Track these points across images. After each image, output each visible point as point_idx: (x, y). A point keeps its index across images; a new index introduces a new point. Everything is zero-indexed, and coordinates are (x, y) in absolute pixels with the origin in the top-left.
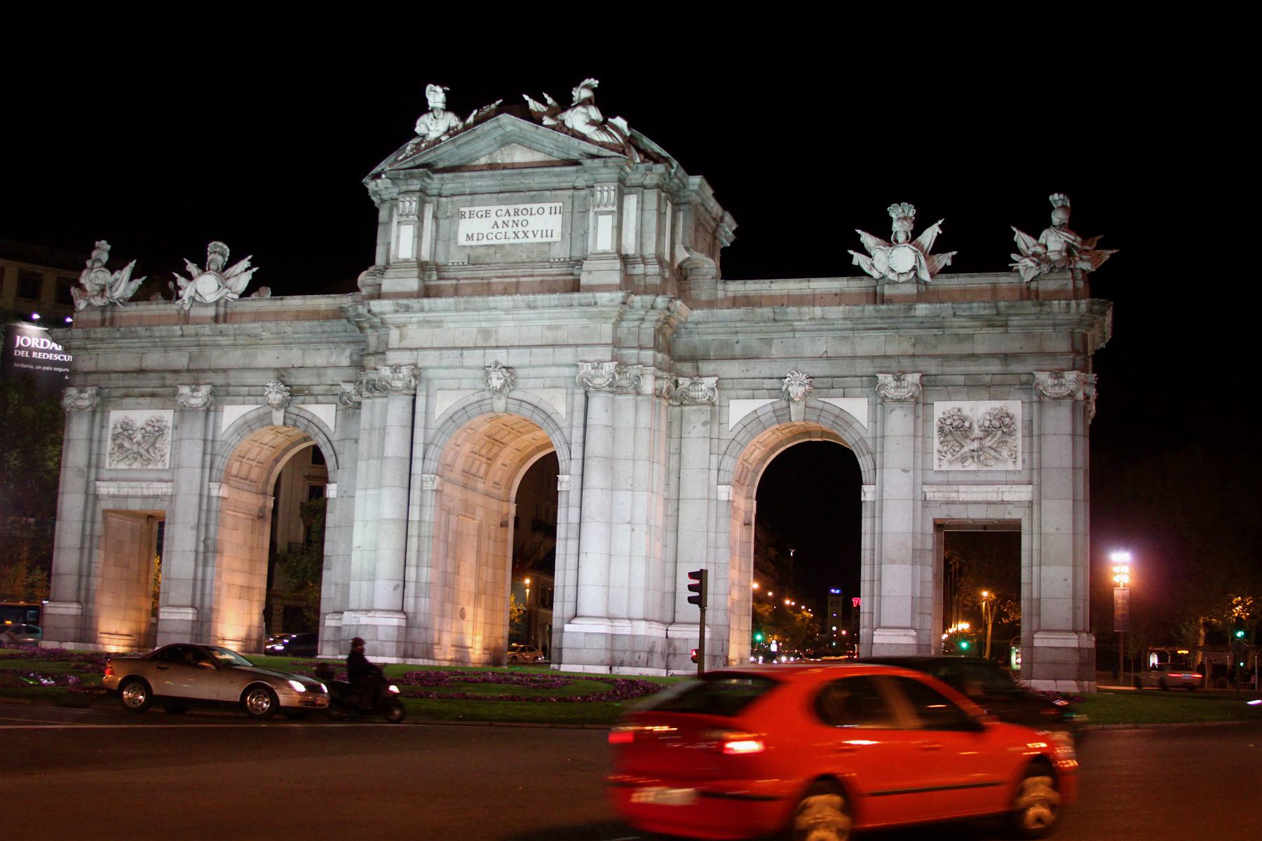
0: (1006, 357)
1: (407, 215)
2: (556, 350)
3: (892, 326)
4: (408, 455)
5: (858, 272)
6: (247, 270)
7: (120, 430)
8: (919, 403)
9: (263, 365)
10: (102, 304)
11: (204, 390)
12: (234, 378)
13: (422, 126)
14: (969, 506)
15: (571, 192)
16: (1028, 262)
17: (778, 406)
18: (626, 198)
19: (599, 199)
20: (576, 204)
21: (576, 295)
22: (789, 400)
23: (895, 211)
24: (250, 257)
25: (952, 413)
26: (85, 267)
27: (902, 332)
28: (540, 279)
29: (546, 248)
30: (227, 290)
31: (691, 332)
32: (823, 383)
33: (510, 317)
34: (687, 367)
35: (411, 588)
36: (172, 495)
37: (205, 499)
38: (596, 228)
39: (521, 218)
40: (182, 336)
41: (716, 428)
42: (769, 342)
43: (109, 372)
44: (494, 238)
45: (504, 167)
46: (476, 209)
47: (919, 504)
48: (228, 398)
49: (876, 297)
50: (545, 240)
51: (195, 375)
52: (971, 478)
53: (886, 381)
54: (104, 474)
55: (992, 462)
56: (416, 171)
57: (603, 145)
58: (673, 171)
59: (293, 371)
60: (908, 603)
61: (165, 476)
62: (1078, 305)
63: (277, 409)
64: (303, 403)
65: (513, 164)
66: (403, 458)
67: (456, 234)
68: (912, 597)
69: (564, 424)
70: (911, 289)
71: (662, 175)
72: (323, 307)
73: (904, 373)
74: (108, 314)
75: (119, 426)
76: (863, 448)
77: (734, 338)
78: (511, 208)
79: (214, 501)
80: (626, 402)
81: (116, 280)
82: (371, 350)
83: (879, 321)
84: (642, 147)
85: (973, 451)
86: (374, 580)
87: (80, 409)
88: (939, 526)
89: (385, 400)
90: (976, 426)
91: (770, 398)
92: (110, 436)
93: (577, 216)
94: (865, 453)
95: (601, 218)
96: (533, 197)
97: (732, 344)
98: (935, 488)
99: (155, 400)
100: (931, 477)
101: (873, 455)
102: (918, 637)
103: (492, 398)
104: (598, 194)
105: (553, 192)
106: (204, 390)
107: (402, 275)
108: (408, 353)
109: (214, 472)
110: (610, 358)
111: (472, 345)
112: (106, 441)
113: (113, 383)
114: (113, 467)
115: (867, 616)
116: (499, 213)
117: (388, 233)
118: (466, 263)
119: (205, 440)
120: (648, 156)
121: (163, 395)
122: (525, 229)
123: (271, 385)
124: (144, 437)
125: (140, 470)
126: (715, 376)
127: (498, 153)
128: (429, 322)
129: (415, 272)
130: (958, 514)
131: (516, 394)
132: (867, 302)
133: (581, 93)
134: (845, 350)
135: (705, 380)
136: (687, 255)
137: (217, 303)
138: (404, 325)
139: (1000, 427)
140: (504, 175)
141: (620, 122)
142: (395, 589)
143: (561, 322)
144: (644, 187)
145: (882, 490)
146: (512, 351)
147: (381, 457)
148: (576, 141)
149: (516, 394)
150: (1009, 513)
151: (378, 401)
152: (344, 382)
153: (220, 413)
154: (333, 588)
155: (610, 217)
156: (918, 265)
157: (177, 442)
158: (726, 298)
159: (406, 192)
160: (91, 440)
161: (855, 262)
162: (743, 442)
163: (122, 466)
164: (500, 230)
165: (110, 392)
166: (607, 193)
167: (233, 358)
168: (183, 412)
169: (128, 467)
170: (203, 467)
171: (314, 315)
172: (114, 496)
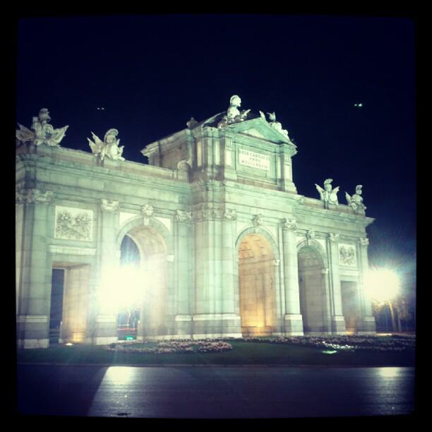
0: (354, 232)
9: (141, 195)
16: (354, 204)
39: (258, 158)
40: (109, 174)
51: (110, 195)
61: (89, 245)
72: (162, 174)
78: (255, 154)
81: (57, 133)
87: (41, 203)
99: (82, 204)
106: (115, 203)
114: (59, 237)
124: (78, 222)
134: (321, 224)
149: (261, 227)
163: (64, 237)
167: (126, 189)
168: (100, 212)
171: (159, 176)
172: (60, 254)
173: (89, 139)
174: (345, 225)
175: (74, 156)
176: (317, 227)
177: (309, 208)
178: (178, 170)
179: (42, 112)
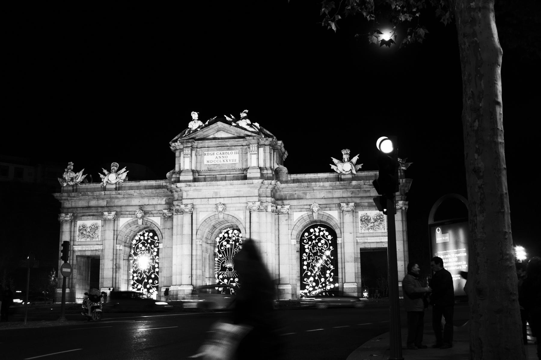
1: (187, 155)
2: (240, 198)
3: (345, 188)
4: (191, 234)
5: (333, 171)
6: (125, 172)
7: (82, 228)
8: (354, 212)
10: (73, 184)
11: (113, 213)
12: (124, 209)
13: (191, 125)
14: (371, 244)
15: (241, 147)
17: (309, 214)
18: (260, 149)
19: (251, 149)
20: (243, 151)
21: (246, 181)
22: (313, 212)
23: (344, 152)
24: (125, 167)
25: (364, 215)
26: (65, 171)
27: (348, 190)
28: (233, 175)
29: (234, 165)
30: (119, 179)
31: (281, 191)
32: (323, 206)
33: (224, 188)
34: (280, 202)
35: (194, 277)
36: (102, 249)
37: (115, 251)
38: (251, 159)
39: (225, 155)
41: (290, 221)
42: (306, 194)
43: (77, 208)
44: (216, 162)
45: (219, 139)
46: (210, 152)
47: (356, 244)
48: (122, 216)
49: (339, 179)
50: (233, 162)
51: (109, 208)
52: (371, 235)
53: (344, 205)
54: (76, 243)
55: (377, 230)
56: (190, 140)
57: (252, 132)
58: (274, 140)
59: (145, 206)
60: (354, 274)
61: (99, 243)
62: (402, 181)
63: (140, 219)
64: (149, 217)
65: (221, 138)
66: (190, 234)
67: (203, 160)
68: (355, 273)
69: (243, 222)
70: (350, 176)
71: (271, 141)
72: (154, 184)
73: (349, 203)
74: (75, 188)
75: (81, 226)
76: (337, 226)
77: (295, 193)
78: (222, 152)
79: (118, 251)
80: (263, 214)
81: (77, 176)
82: (176, 198)
83: (340, 186)
84: (263, 132)
85: (371, 226)
86: (182, 275)
87: (66, 221)
88: (361, 249)
89: (182, 215)
90: (372, 219)
91: (307, 211)
92: (78, 230)
93: (243, 154)
94: (338, 228)
95: (252, 155)
96: (229, 148)
97: (294, 195)
98: (360, 238)
99: (94, 217)
100: (359, 235)
101: (340, 228)
102: (357, 285)
103: (218, 214)
104: (251, 148)
105: (235, 147)
106: (113, 213)
107: (187, 174)
108: (190, 200)
109: (118, 241)
110: (258, 200)
111: (212, 197)
112: (76, 231)
113: (78, 212)
114: (79, 240)
115: (341, 279)
116: (218, 154)
117: (179, 160)
118: (207, 170)
119: (114, 230)
120: (267, 136)
121: (100, 215)
122: (227, 159)
123: (137, 211)
124: (91, 230)
125: (90, 241)
126: (289, 205)
127: (216, 134)
128: (197, 190)
129: (191, 173)
130: (368, 246)
131: (226, 213)
132: (336, 181)
133: (243, 115)
134: (330, 196)
135: (286, 206)
136: (278, 166)
137: (116, 183)
138: (188, 191)
139: (380, 219)
140: (219, 141)
141: (257, 124)
142: (189, 278)
143: (241, 189)
144: (265, 145)
145: (344, 239)
146: (225, 199)
147: (182, 234)
148: (244, 131)
149: (226, 213)
150: (384, 245)
151: (179, 216)
152: (164, 209)
153: (119, 221)
154: (163, 278)
155: (255, 155)
156: (352, 169)
157: (104, 231)
158: (291, 180)
159: (186, 147)
160: (71, 232)
161: (332, 168)
162: (298, 226)
164: (218, 159)
165: (77, 215)
166: (254, 147)
167: (123, 202)
168: (105, 221)
169: (85, 240)
170: (114, 239)
171: (151, 187)
172: (80, 251)
173: (100, 174)
174: (366, 191)
175: (89, 187)
176: (323, 200)
177: (306, 184)
178: (167, 178)
179: (70, 165)
